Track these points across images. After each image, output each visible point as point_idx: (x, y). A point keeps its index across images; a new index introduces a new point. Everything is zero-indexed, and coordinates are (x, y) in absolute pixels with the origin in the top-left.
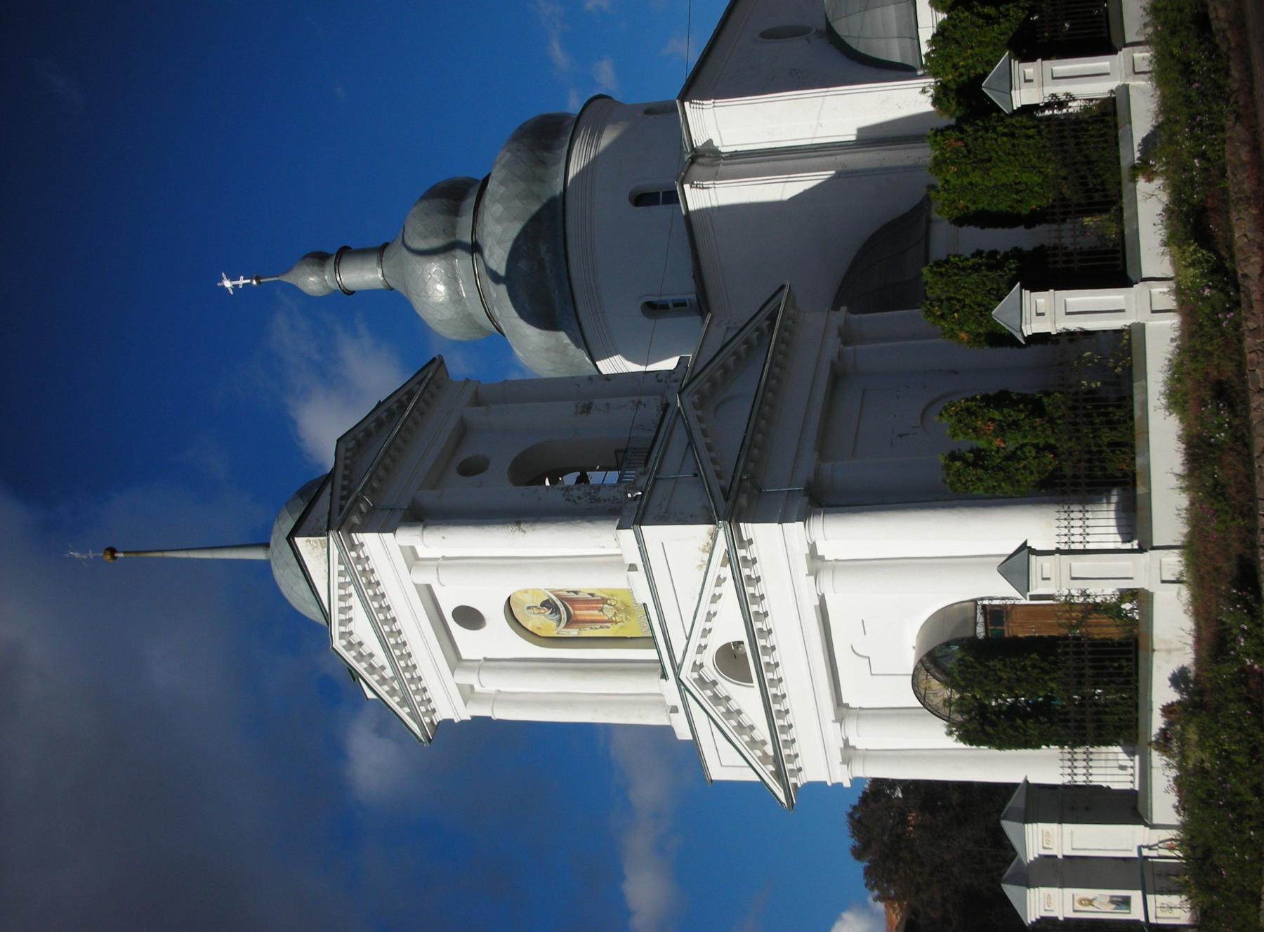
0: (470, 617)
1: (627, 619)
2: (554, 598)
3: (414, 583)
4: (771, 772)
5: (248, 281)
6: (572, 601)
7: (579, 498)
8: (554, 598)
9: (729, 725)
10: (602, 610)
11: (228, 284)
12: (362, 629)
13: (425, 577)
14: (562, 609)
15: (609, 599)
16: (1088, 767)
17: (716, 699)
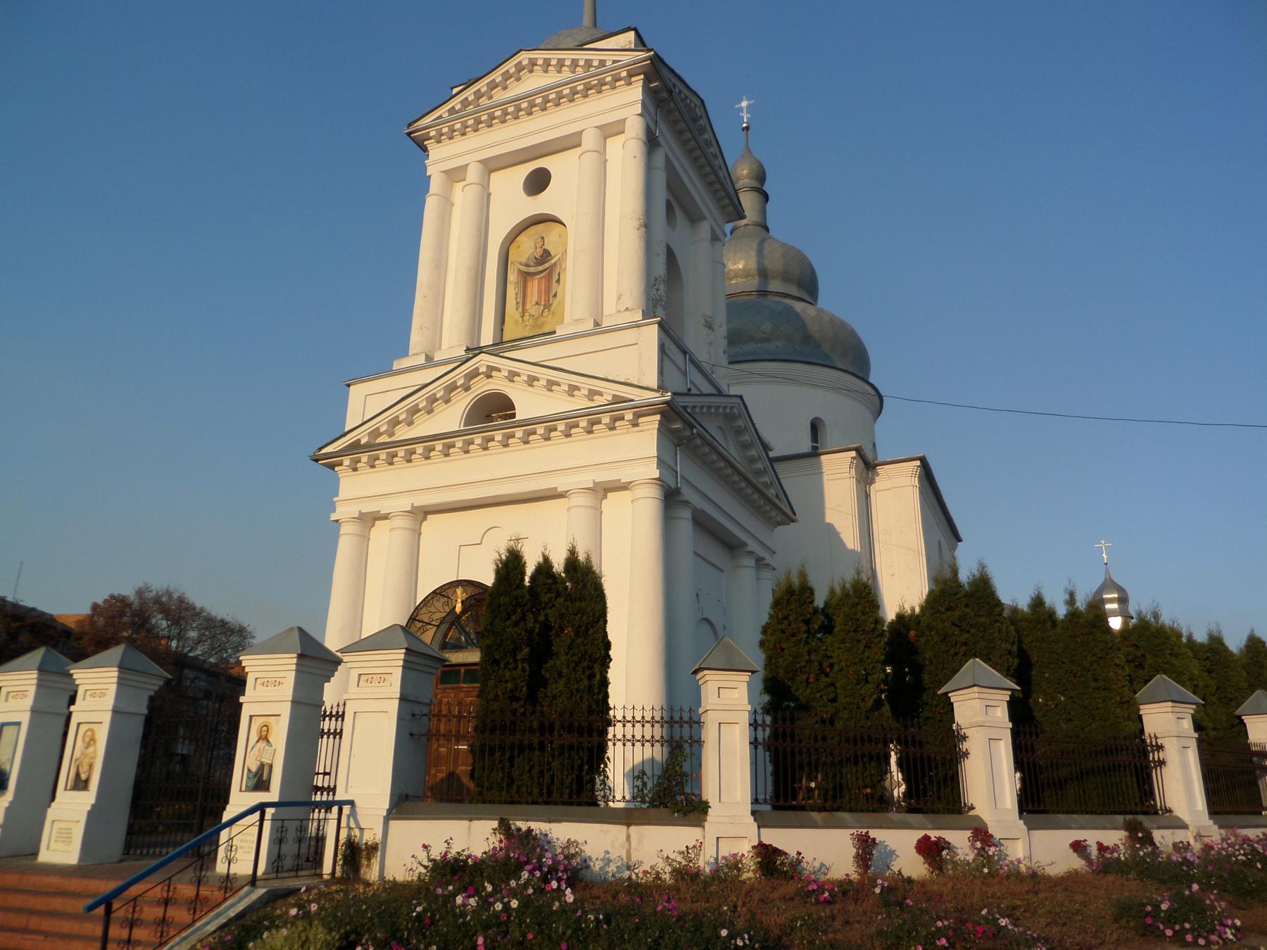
0: (538, 182)
1: (526, 326)
2: (553, 261)
4: (359, 440)
6: (549, 277)
7: (658, 290)
8: (553, 261)
9: (420, 399)
10: (537, 304)
11: (744, 104)
12: (534, 82)
13: (589, 140)
14: (540, 268)
15: (549, 310)
17: (452, 388)
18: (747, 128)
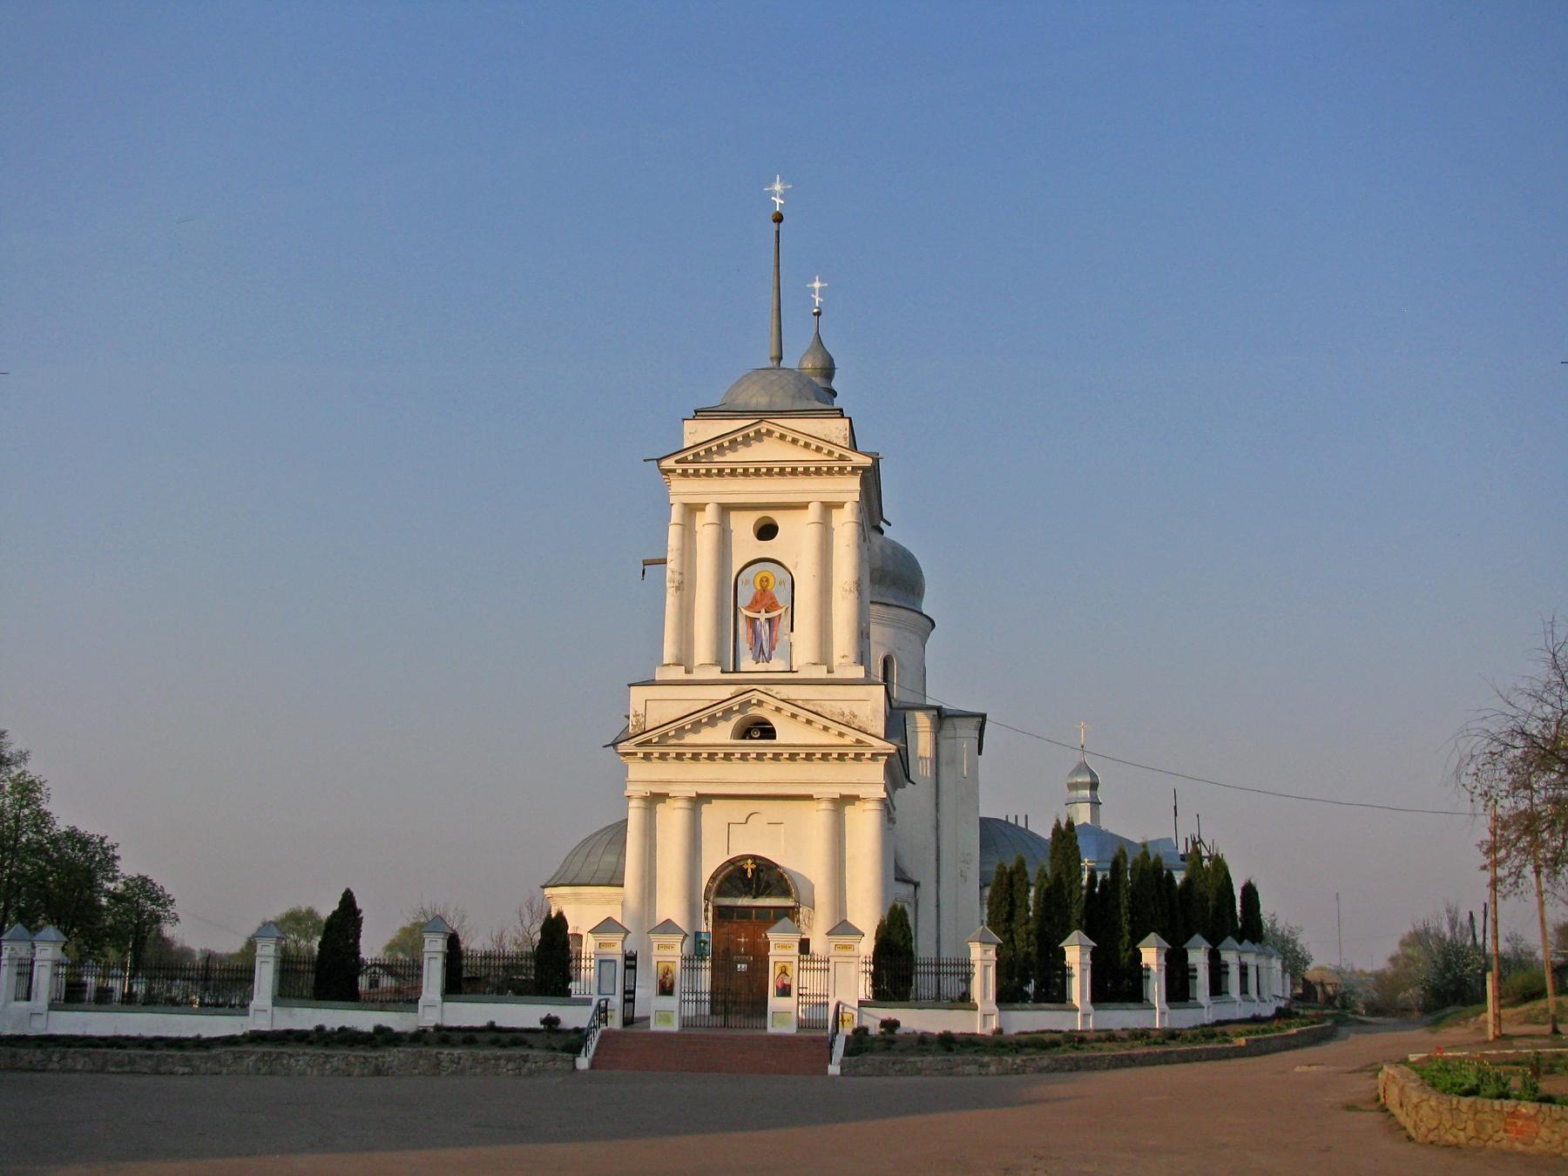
0: (767, 531)
3: (809, 503)
5: (817, 304)
16: (821, 970)
18: (818, 314)
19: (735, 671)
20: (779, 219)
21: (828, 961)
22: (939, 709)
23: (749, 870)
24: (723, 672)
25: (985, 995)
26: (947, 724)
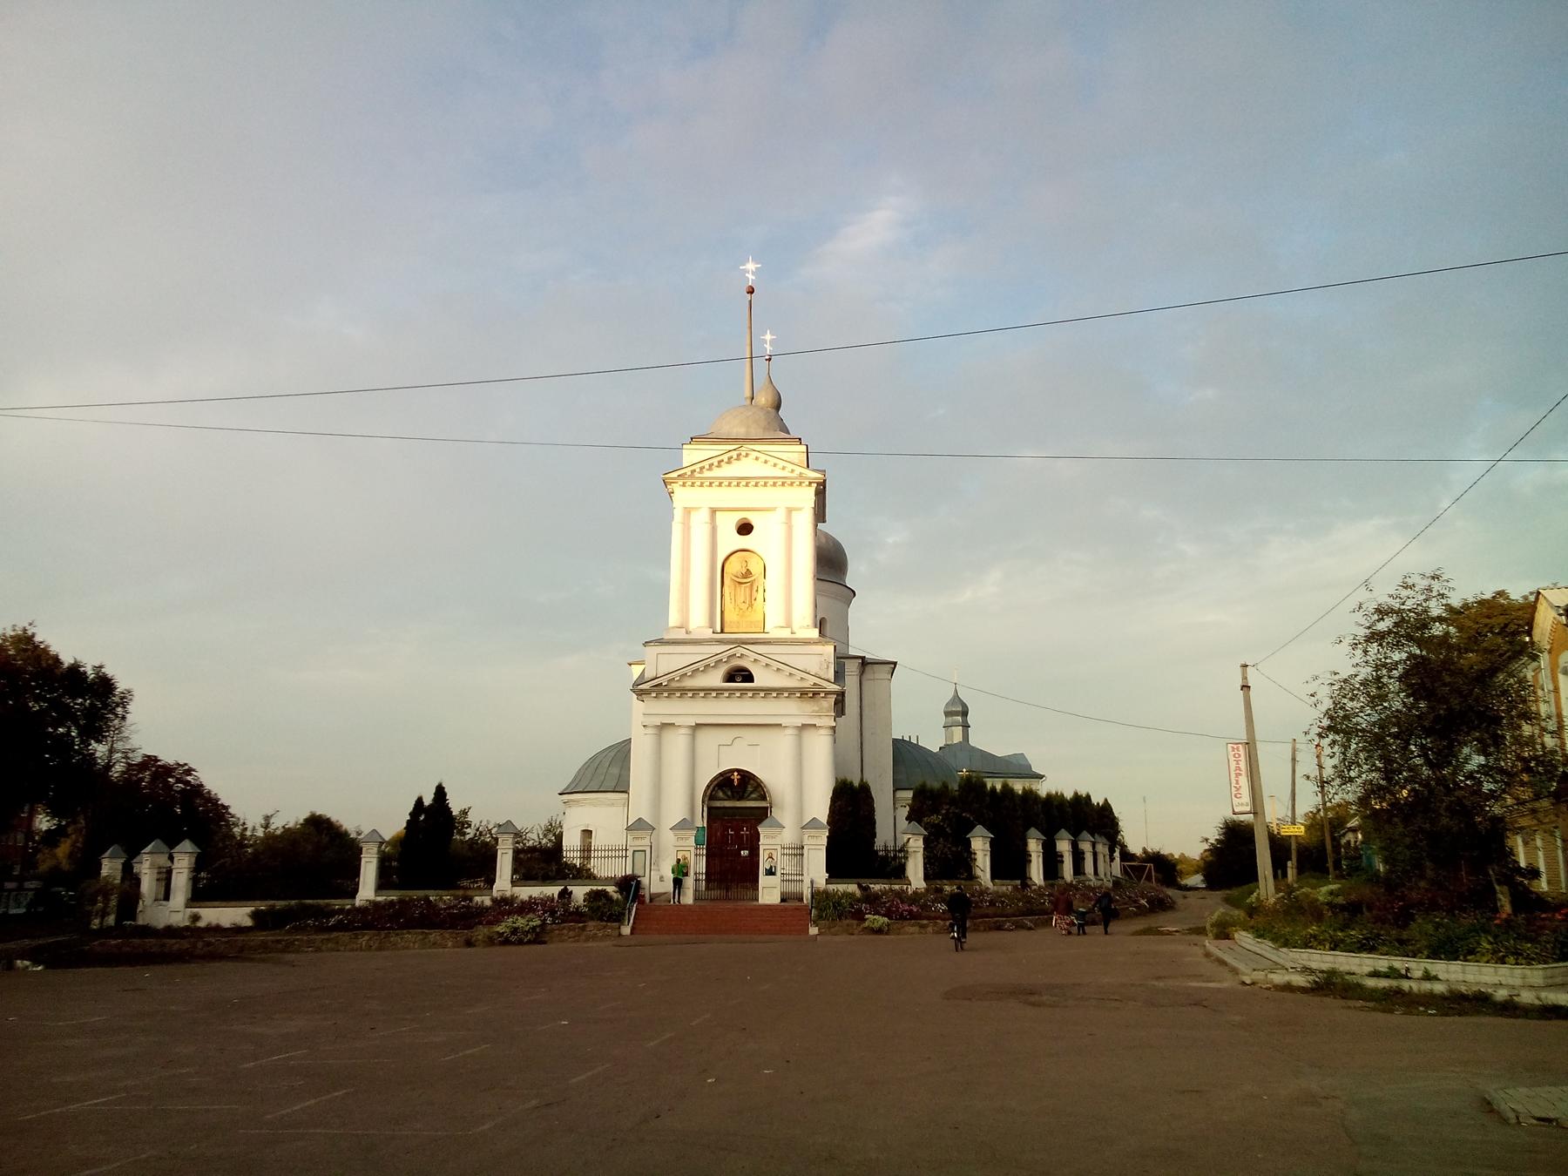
0: (745, 529)
2: (753, 578)
6: (752, 585)
8: (753, 578)
9: (701, 666)
19: (722, 632)
20: (751, 291)
21: (803, 847)
22: (863, 658)
23: (736, 780)
24: (713, 632)
25: (916, 874)
26: (868, 668)
